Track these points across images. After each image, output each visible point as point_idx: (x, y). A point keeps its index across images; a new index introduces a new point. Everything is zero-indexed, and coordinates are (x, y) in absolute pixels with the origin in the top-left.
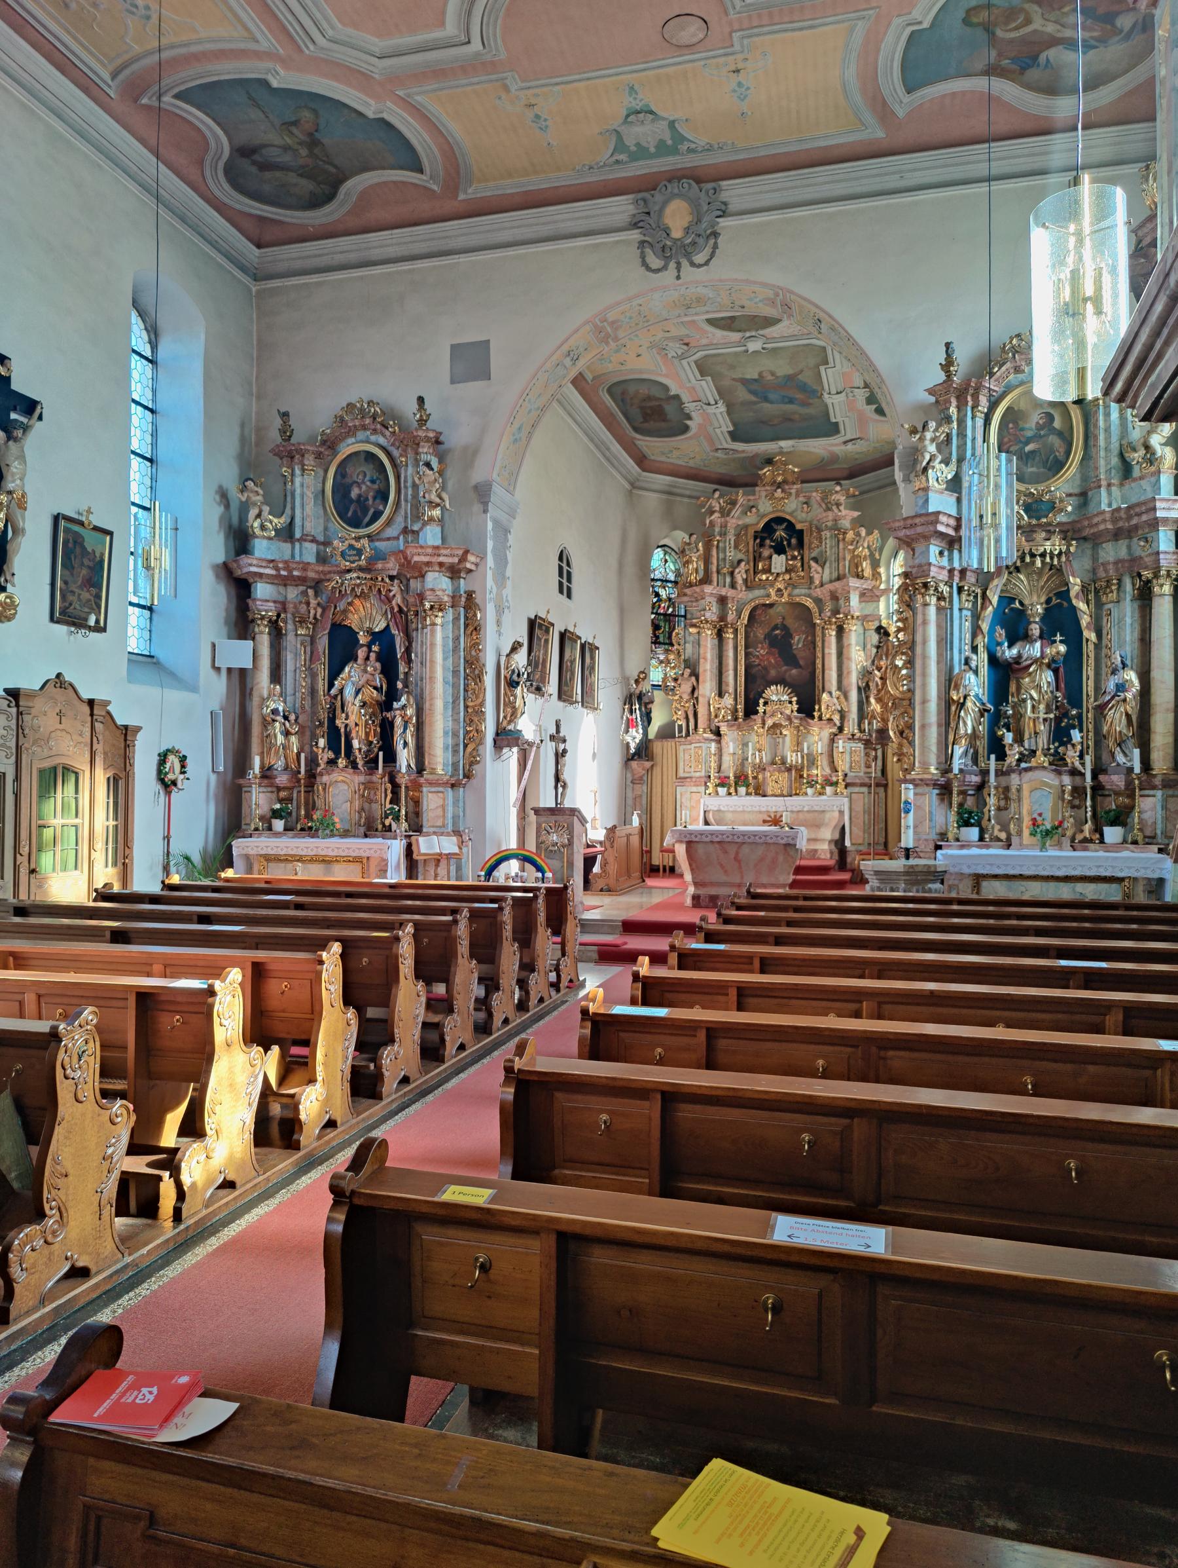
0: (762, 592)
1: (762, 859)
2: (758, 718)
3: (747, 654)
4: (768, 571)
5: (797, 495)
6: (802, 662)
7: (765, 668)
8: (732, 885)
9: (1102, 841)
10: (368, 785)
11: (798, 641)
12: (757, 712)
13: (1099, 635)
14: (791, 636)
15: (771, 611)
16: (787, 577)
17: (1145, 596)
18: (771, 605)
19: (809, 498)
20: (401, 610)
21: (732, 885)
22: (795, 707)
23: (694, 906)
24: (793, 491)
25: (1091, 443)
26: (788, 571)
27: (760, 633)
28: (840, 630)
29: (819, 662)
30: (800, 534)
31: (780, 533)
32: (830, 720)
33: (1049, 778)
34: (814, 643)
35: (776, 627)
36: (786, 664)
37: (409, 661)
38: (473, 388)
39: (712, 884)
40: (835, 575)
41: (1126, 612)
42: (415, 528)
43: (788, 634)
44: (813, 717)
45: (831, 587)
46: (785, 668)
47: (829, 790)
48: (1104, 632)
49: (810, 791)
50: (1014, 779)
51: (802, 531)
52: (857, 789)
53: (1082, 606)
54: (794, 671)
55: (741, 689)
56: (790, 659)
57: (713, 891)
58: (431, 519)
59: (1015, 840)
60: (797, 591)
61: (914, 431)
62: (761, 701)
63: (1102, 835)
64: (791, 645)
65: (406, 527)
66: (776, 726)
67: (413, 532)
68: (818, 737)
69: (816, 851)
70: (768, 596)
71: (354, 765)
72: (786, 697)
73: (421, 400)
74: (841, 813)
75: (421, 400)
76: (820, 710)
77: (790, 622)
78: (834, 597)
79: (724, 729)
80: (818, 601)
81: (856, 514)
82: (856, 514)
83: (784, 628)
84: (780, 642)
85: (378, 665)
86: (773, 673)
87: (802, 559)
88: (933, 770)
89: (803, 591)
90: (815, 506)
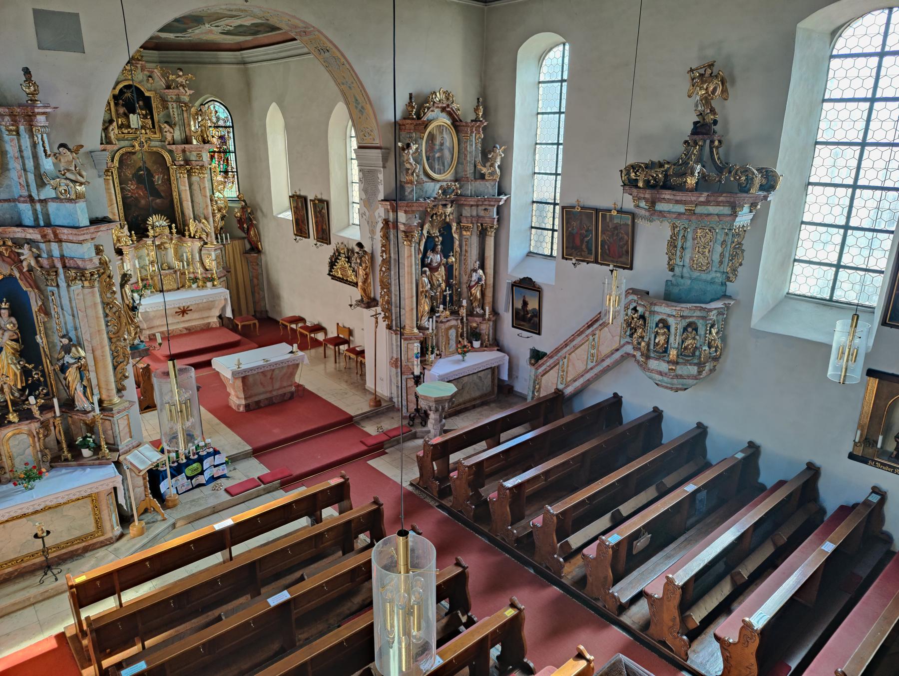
0: (126, 143)
1: (285, 374)
2: (149, 241)
3: (122, 189)
4: (129, 126)
5: (142, 70)
6: (162, 194)
7: (136, 199)
8: (266, 392)
9: (472, 346)
10: (45, 425)
11: (158, 179)
12: (148, 236)
13: (461, 250)
14: (153, 176)
15: (134, 157)
16: (143, 131)
17: (483, 234)
18: (134, 153)
19: (152, 72)
20: (31, 269)
21: (266, 392)
22: (174, 231)
23: (247, 411)
24: (139, 66)
25: (462, 156)
26: (142, 127)
27: (129, 173)
28: (189, 173)
29: (175, 194)
30: (147, 102)
31: (128, 95)
32: (200, 238)
33: (453, 323)
34: (169, 179)
35: (140, 169)
36: (152, 196)
37: (47, 313)
38: (66, 58)
39: (255, 395)
40: (183, 136)
41: (475, 241)
42: (42, 198)
43: (150, 175)
44: (184, 236)
45: (183, 146)
46: (151, 198)
47: (209, 284)
48: (464, 249)
49: (194, 286)
50: (440, 325)
51: (149, 98)
52: (222, 279)
53: (456, 236)
54: (158, 201)
55: (122, 215)
56: (154, 192)
57: (256, 399)
58: (79, 196)
59: (443, 354)
60: (153, 143)
61: (404, 149)
62: (150, 228)
63: (471, 343)
64: (153, 182)
65: (30, 196)
66: (162, 244)
67: (41, 201)
68: (191, 246)
69: (209, 323)
70: (133, 146)
71: (26, 415)
72: (165, 223)
73: (27, 71)
74: (226, 299)
75: (27, 71)
76: (189, 230)
77: (149, 165)
78: (184, 151)
79: (125, 250)
80: (171, 152)
81: (192, 92)
82: (192, 92)
83: (148, 170)
84: (144, 178)
85: (13, 319)
86: (143, 202)
87: (152, 119)
88: (416, 330)
89: (157, 144)
90: (157, 79)
